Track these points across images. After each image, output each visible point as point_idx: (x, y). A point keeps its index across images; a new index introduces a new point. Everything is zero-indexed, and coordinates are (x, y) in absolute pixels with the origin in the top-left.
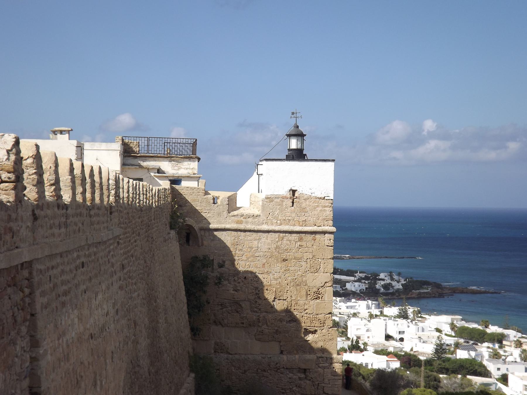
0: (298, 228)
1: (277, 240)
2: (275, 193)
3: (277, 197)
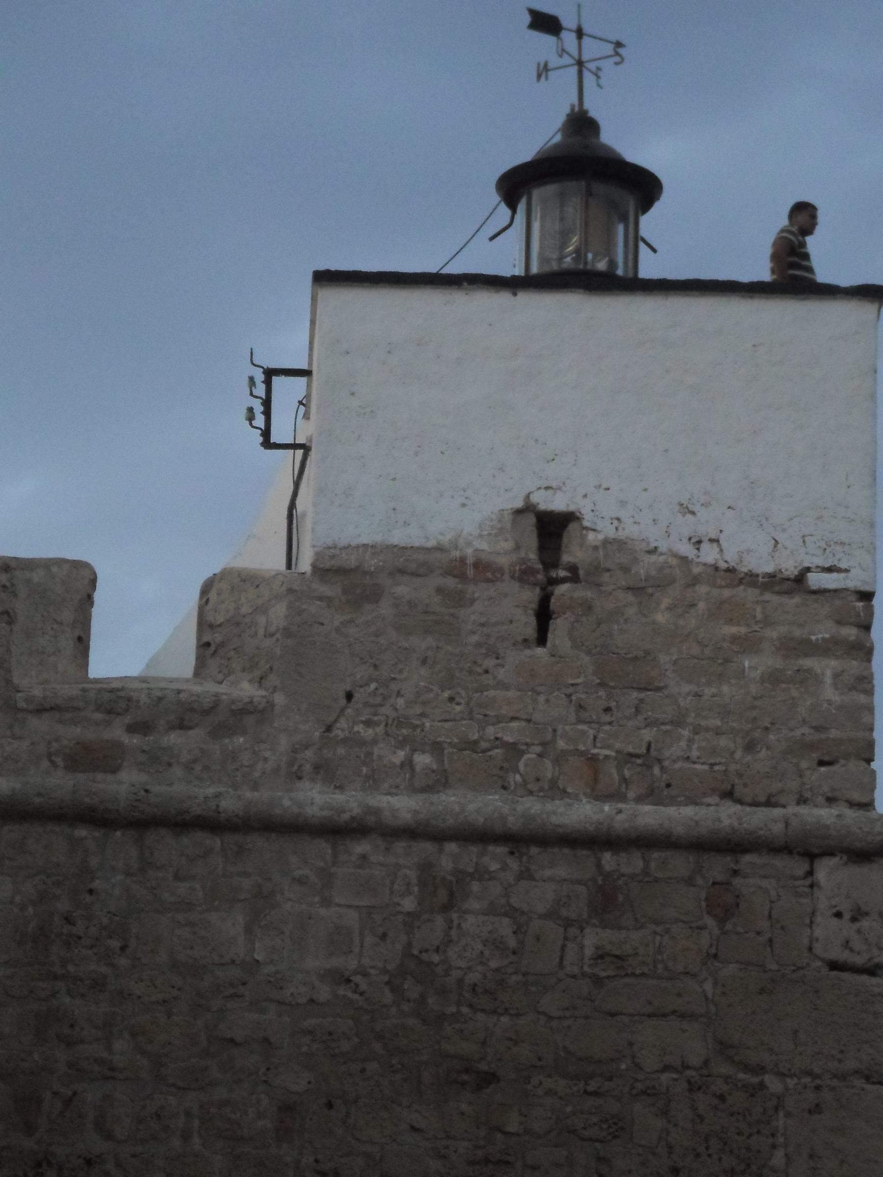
0: (581, 813)
2: (398, 537)
3: (408, 563)
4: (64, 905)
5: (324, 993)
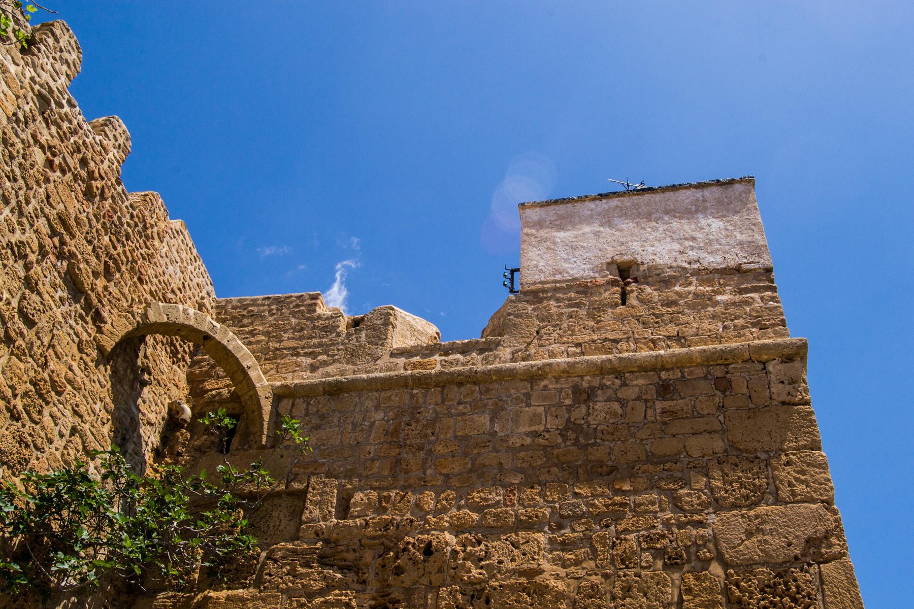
4: (406, 419)
5: (528, 441)
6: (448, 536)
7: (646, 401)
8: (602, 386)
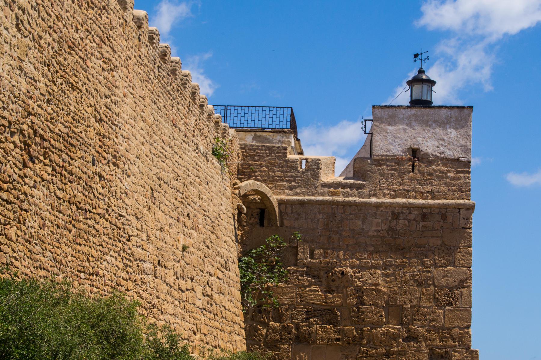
1: (390, 218)
4: (331, 219)
5: (375, 234)
6: (349, 270)
7: (417, 221)
8: (402, 213)
